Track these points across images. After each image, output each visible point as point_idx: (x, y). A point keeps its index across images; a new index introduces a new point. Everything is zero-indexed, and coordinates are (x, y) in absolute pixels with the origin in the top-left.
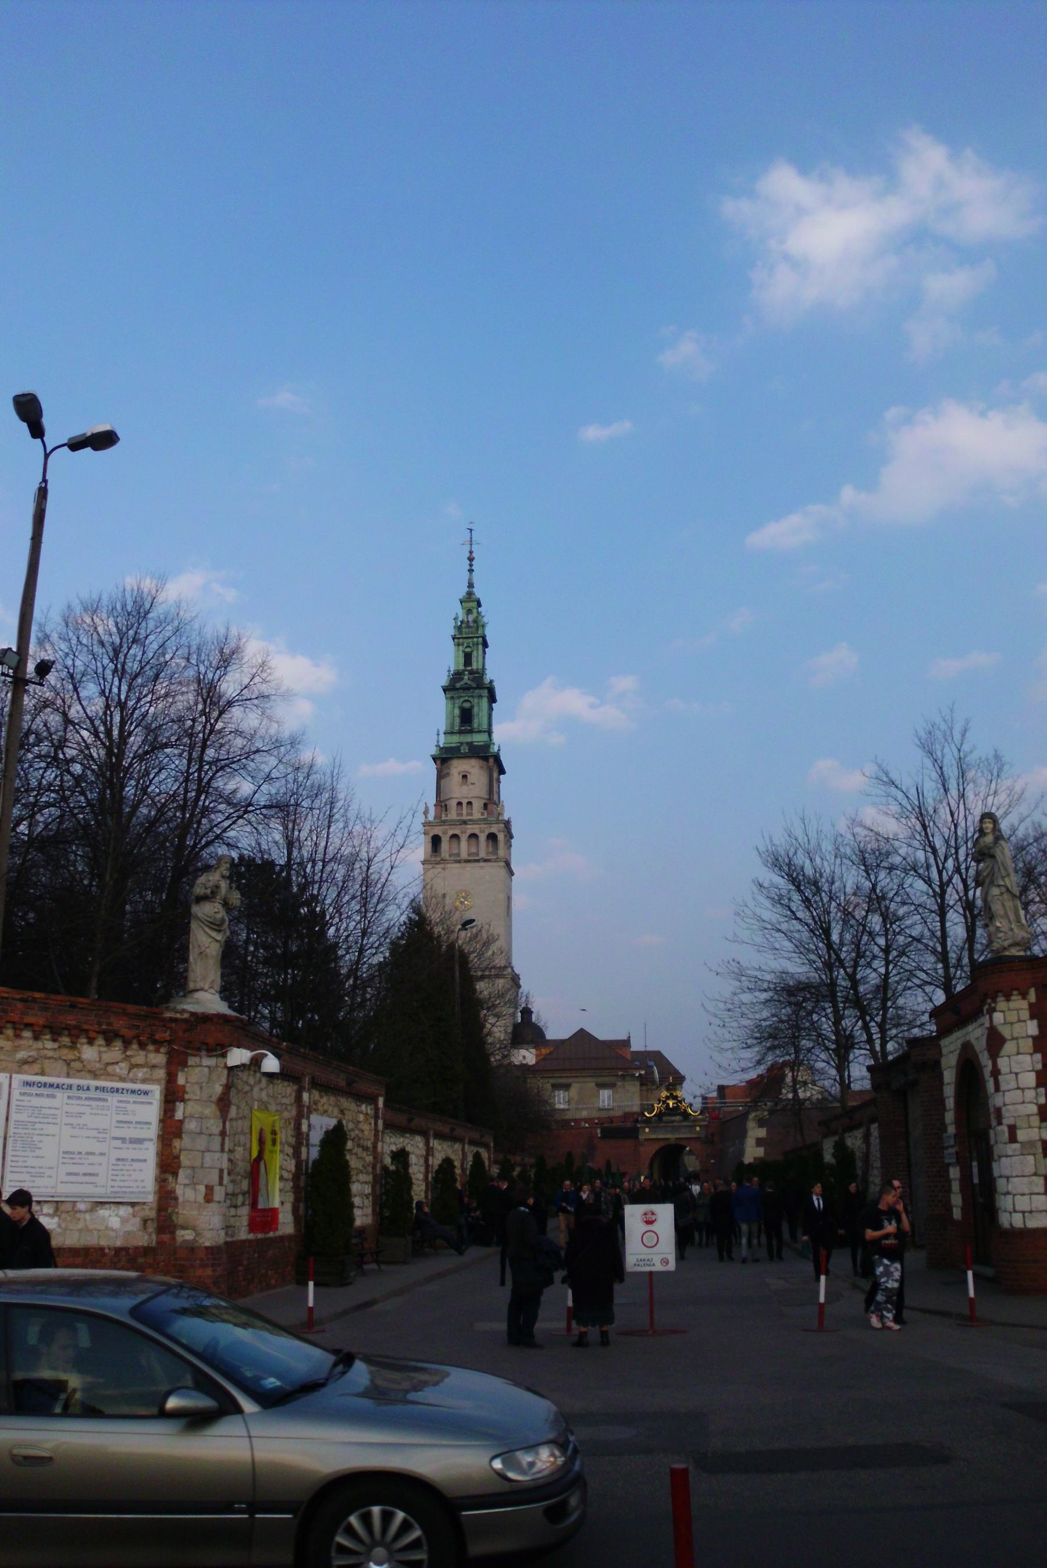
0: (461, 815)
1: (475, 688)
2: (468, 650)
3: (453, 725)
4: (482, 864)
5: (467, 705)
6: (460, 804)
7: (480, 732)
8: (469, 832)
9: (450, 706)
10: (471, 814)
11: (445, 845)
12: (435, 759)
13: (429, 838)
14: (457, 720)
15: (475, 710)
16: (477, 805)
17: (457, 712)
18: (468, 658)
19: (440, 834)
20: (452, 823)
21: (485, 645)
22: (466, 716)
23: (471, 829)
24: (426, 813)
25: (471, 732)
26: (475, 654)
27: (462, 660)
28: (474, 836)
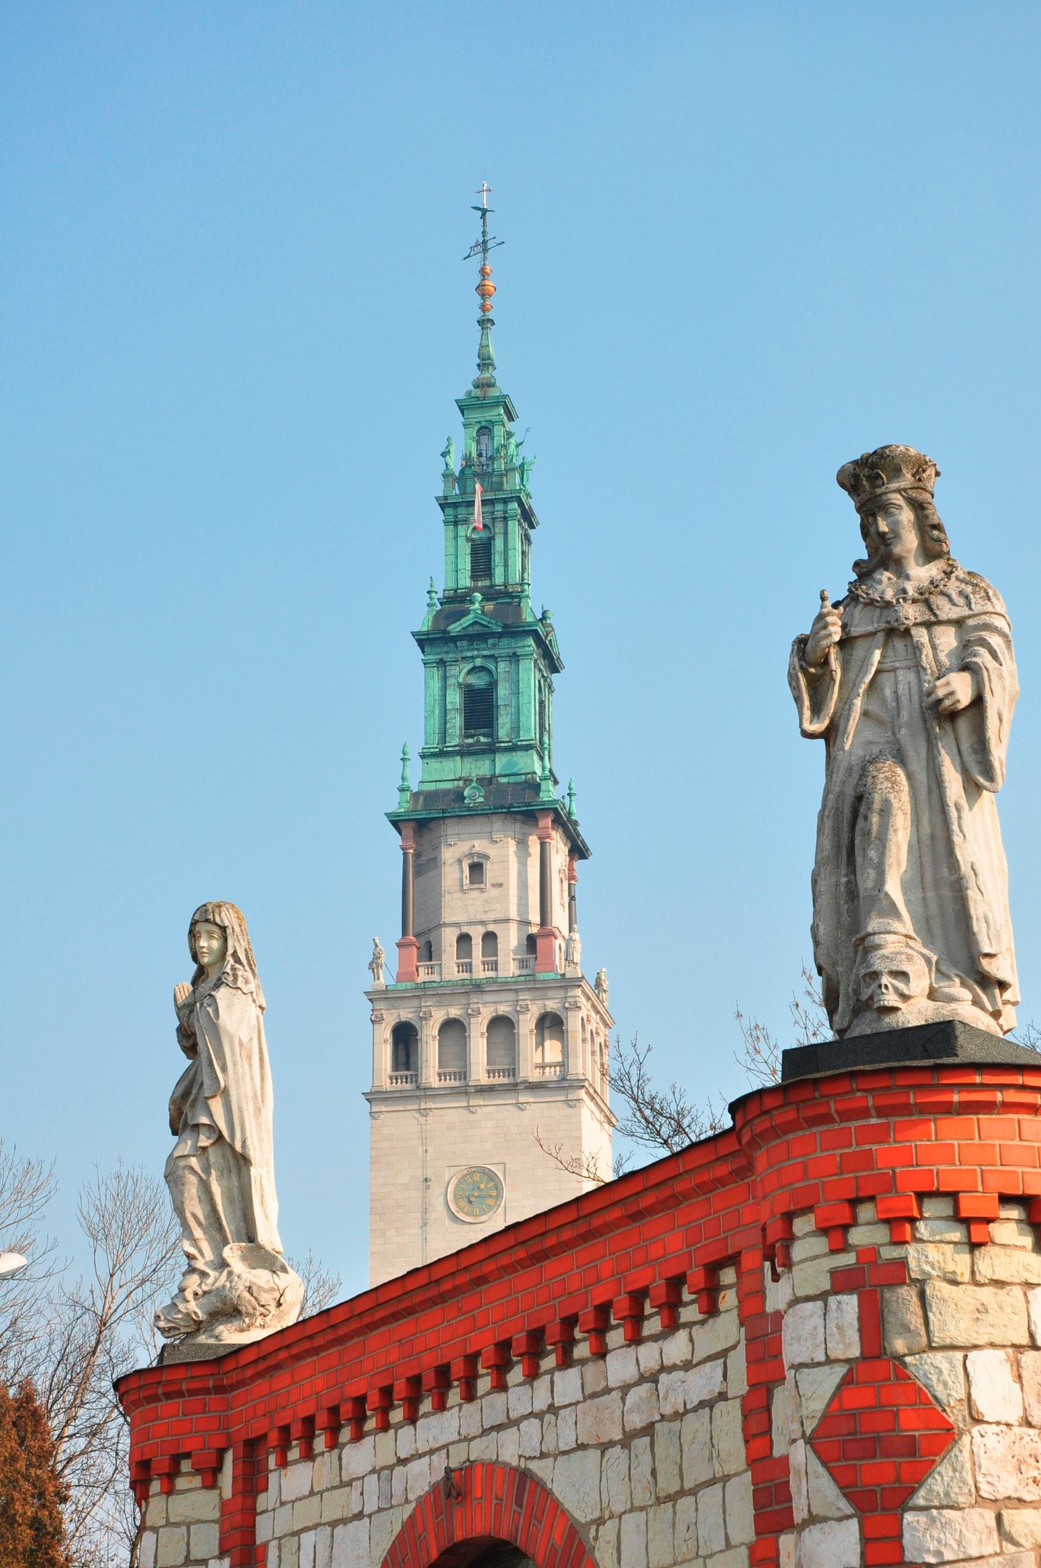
0: (469, 968)
1: (500, 636)
5: (478, 681)
6: (464, 939)
7: (514, 748)
9: (436, 684)
10: (495, 966)
12: (397, 822)
13: (386, 1033)
14: (457, 721)
15: (503, 692)
16: (511, 939)
18: (482, 556)
20: (442, 992)
21: (528, 517)
22: (480, 709)
25: (492, 750)
26: (498, 544)
27: (466, 563)
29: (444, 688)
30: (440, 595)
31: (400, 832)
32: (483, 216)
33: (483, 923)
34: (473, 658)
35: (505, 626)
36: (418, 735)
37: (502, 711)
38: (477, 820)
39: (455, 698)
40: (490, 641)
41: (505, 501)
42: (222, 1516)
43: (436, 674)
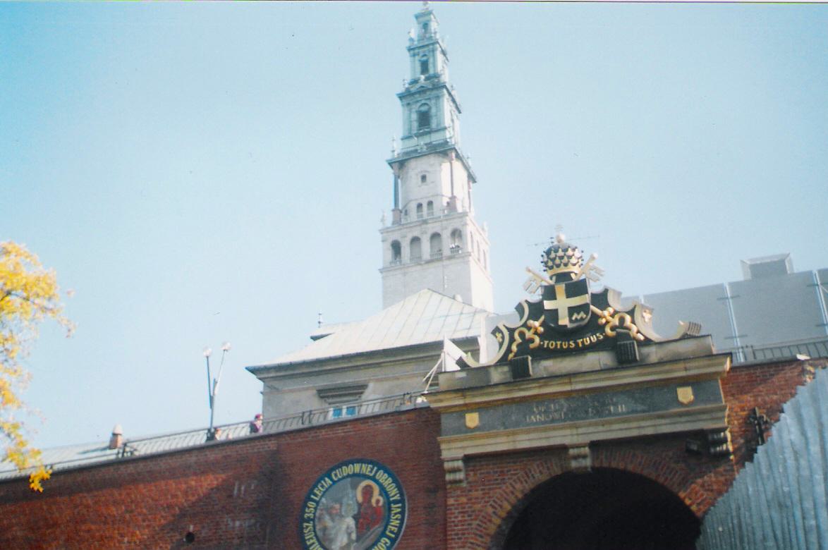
0: (422, 216)
1: (432, 89)
2: (425, 58)
3: (410, 130)
5: (424, 109)
6: (420, 206)
9: (407, 112)
11: (406, 250)
12: (391, 164)
13: (388, 245)
14: (415, 125)
17: (414, 116)
18: (425, 67)
19: (400, 239)
22: (424, 119)
23: (432, 228)
24: (383, 220)
25: (430, 133)
27: (418, 69)
28: (436, 236)
29: (410, 114)
31: (392, 167)
33: (426, 197)
35: (434, 85)
36: (399, 131)
41: (433, 44)
43: (406, 108)
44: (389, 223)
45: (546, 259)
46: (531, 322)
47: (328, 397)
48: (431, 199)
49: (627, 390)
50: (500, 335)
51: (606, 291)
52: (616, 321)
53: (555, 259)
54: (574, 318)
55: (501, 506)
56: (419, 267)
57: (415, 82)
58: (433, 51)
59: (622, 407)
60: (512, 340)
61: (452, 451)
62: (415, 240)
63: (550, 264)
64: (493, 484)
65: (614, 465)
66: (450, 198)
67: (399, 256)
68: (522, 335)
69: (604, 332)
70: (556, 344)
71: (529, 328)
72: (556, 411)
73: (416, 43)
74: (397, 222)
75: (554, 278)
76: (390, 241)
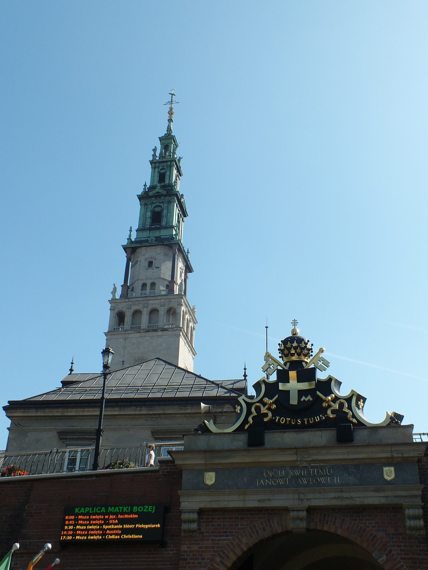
1: (165, 196)
2: (163, 171)
4: (160, 333)
5: (158, 209)
6: (144, 285)
8: (150, 307)
11: (128, 319)
12: (125, 248)
14: (149, 221)
15: (165, 212)
18: (162, 177)
19: (124, 310)
23: (154, 303)
25: (159, 229)
27: (157, 178)
28: (154, 312)
29: (146, 211)
30: (148, 186)
31: (126, 252)
32: (172, 97)
34: (156, 203)
37: (164, 217)
38: (153, 247)
39: (149, 214)
40: (162, 198)
42: (6, 451)
44: (118, 296)
45: (282, 348)
46: (266, 400)
47: (66, 439)
48: (156, 281)
49: (343, 467)
50: (239, 408)
51: (330, 379)
52: (336, 406)
53: (290, 348)
54: (302, 400)
55: (228, 557)
56: (138, 335)
57: (152, 188)
58: (171, 167)
59: (337, 479)
60: (249, 412)
61: (190, 503)
62: (137, 313)
63: (286, 352)
64: (223, 536)
65: (325, 529)
66: (170, 282)
67: (122, 324)
68: (258, 409)
69: (327, 414)
70: (286, 420)
71: (264, 404)
72: (282, 478)
73: (157, 158)
74: (125, 295)
75: (288, 364)
76: (116, 310)
